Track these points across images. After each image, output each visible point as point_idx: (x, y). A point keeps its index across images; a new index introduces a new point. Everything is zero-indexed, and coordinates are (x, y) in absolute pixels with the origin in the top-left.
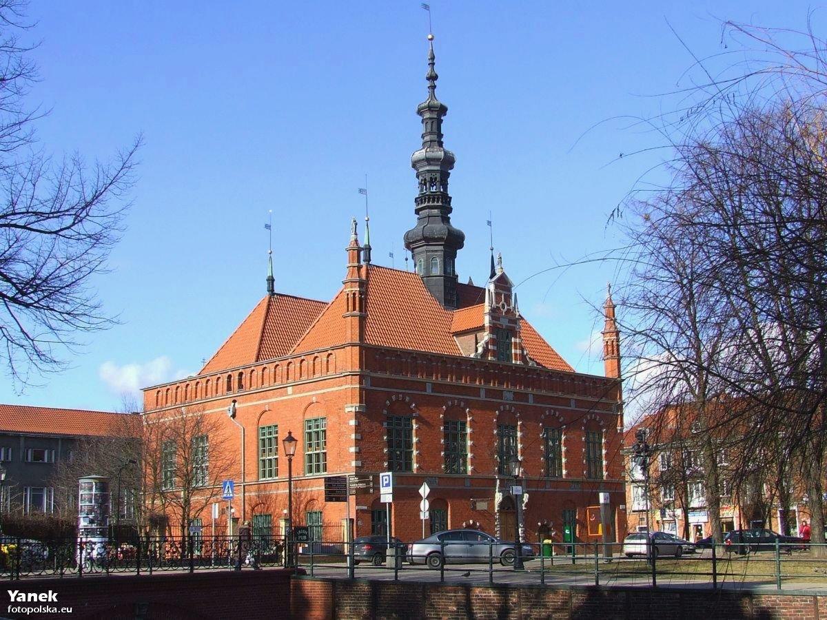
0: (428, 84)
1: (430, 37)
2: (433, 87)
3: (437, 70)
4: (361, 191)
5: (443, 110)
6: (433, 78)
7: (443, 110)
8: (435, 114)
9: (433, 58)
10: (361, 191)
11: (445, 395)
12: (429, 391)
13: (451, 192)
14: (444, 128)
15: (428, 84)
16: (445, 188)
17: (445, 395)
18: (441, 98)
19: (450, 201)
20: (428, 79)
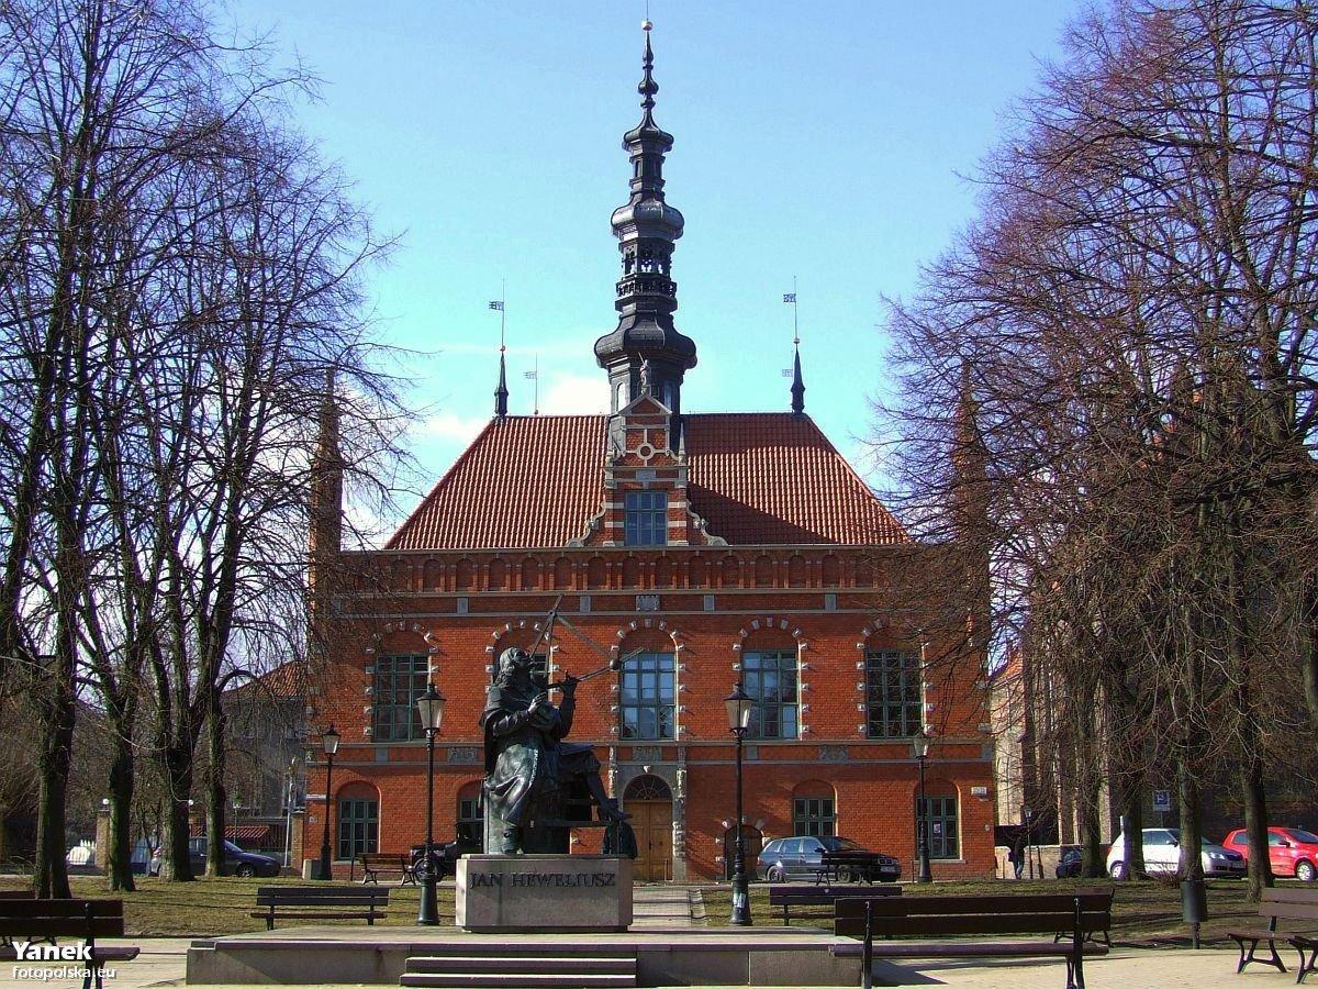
0: (643, 98)
1: (644, 24)
2: (649, 105)
3: (655, 77)
4: (493, 305)
5: (666, 141)
6: (649, 89)
7: (666, 141)
8: (650, 147)
9: (649, 57)
10: (493, 305)
11: (497, 615)
12: (462, 611)
13: (674, 276)
14: (667, 171)
15: (643, 98)
16: (667, 268)
17: (497, 615)
18: (663, 122)
19: (675, 289)
20: (641, 91)
